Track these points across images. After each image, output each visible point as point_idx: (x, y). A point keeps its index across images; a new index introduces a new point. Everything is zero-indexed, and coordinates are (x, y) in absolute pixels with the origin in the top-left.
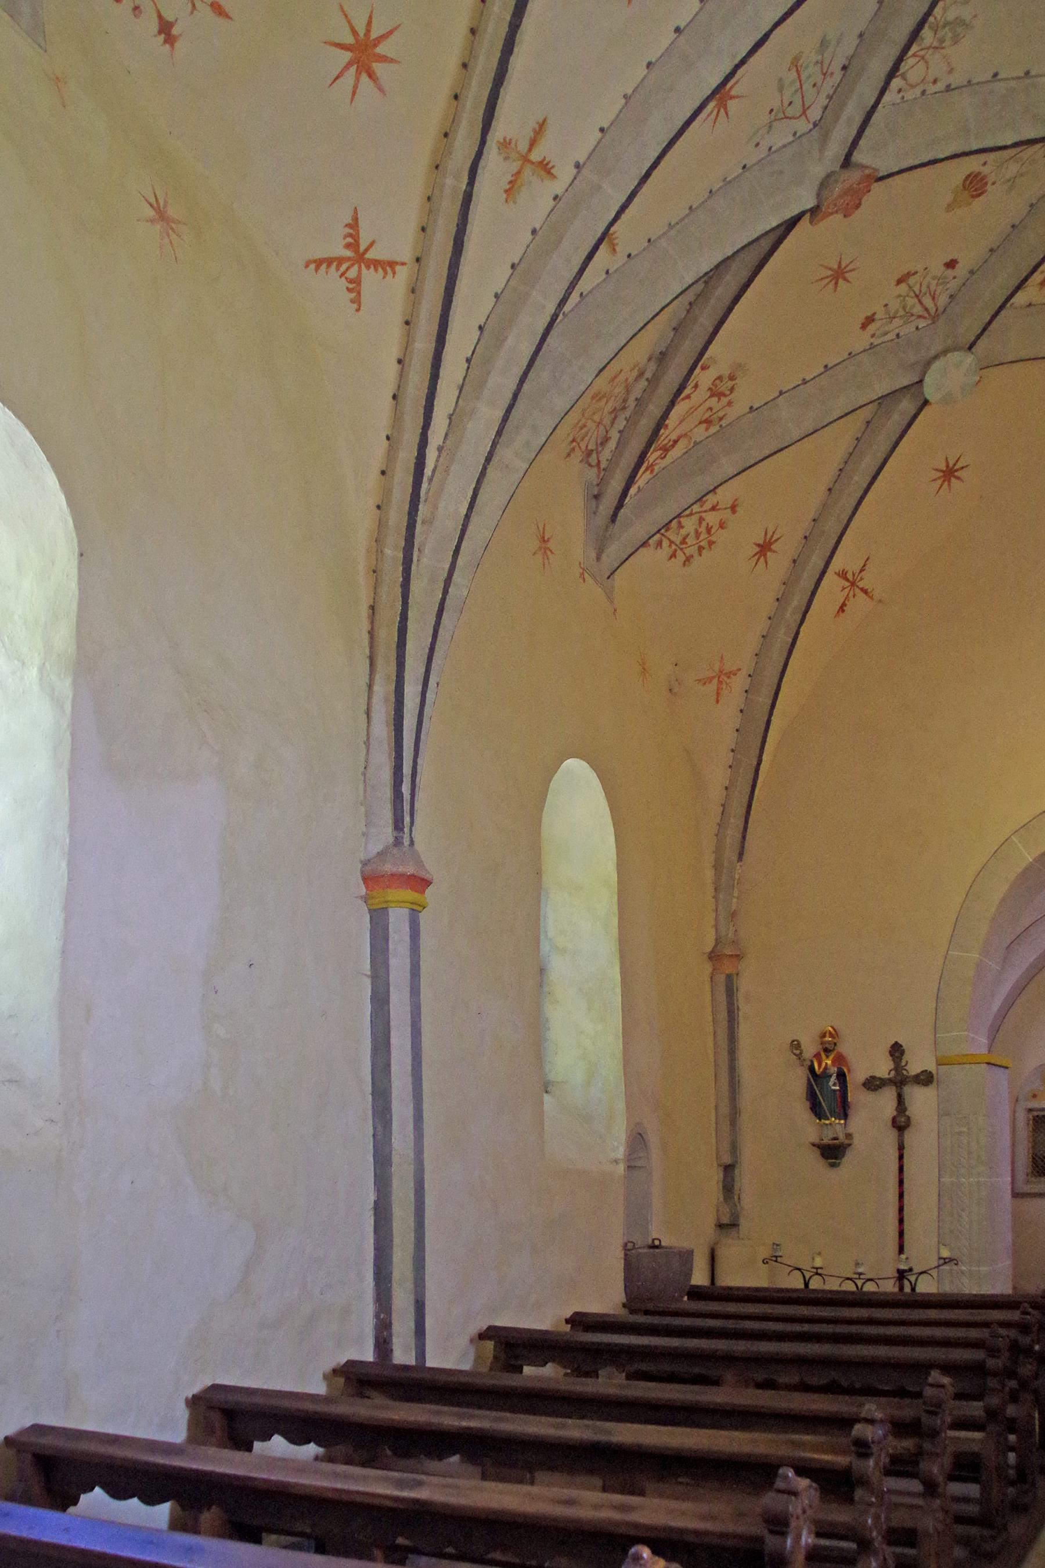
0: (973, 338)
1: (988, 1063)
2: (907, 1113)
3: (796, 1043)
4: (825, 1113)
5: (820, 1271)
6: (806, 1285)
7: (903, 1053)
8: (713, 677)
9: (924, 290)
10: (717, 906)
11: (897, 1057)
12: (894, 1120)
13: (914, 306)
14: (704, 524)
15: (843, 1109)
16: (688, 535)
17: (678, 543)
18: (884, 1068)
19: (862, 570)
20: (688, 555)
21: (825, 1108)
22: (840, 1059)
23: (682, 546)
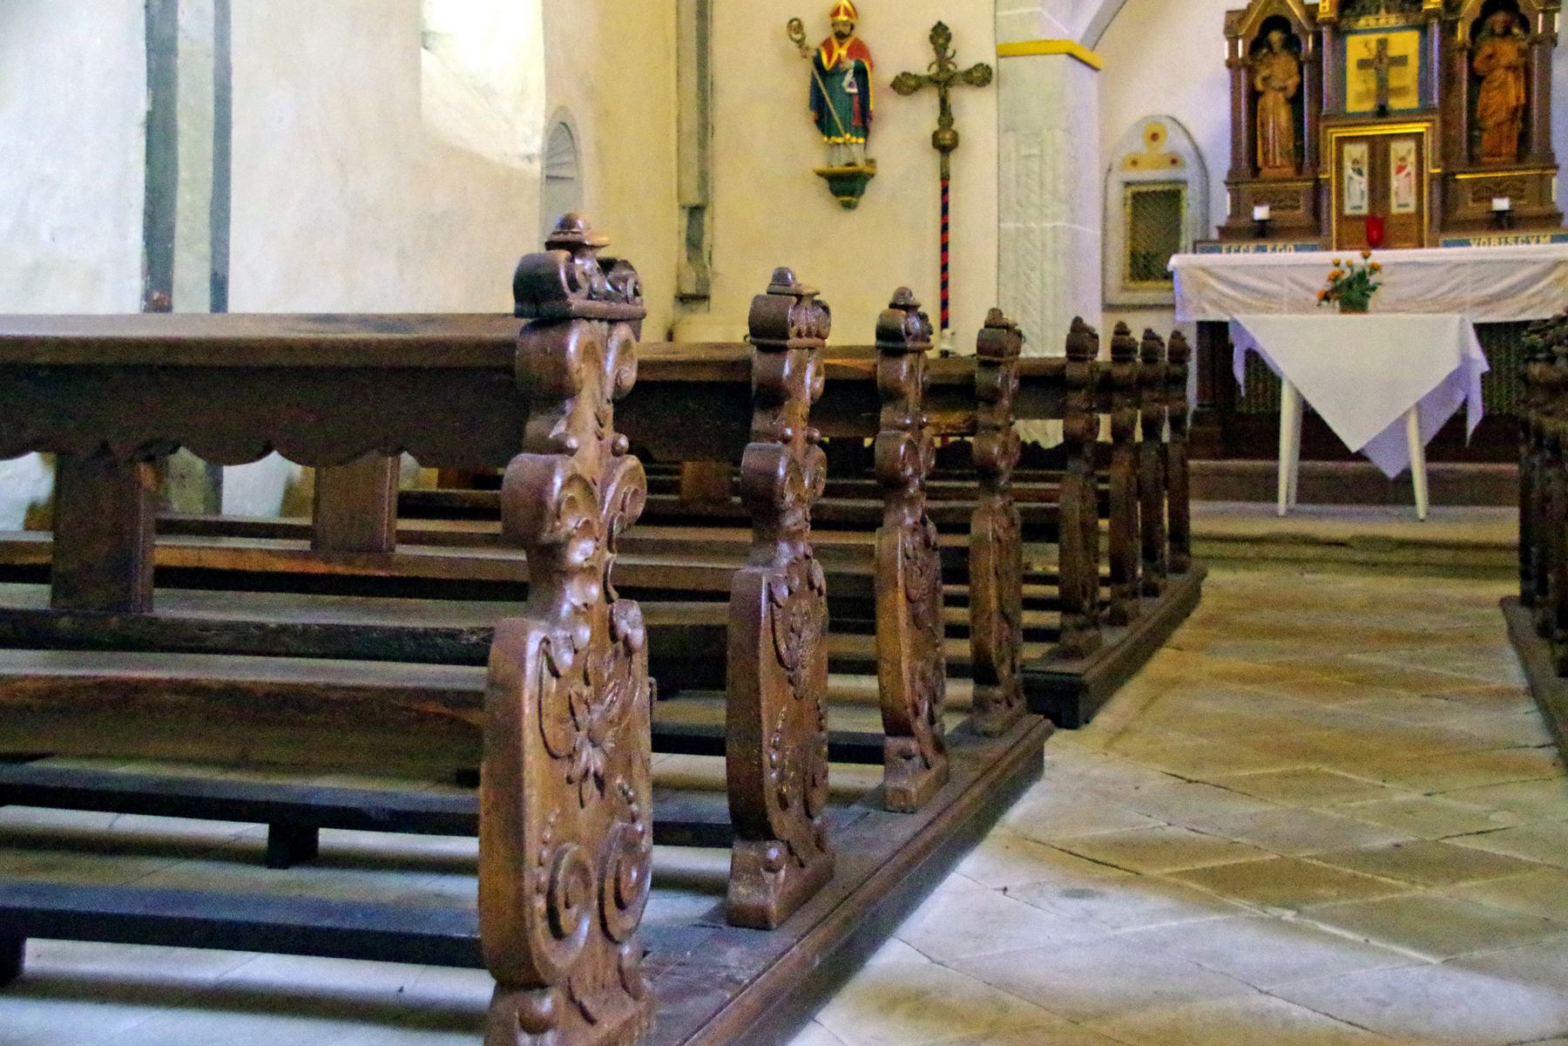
1: (1071, 55)
2: (954, 127)
3: (795, 23)
4: (838, 129)
7: (948, 38)
11: (941, 45)
12: (935, 135)
15: (863, 121)
18: (921, 61)
21: (837, 118)
22: (859, 50)
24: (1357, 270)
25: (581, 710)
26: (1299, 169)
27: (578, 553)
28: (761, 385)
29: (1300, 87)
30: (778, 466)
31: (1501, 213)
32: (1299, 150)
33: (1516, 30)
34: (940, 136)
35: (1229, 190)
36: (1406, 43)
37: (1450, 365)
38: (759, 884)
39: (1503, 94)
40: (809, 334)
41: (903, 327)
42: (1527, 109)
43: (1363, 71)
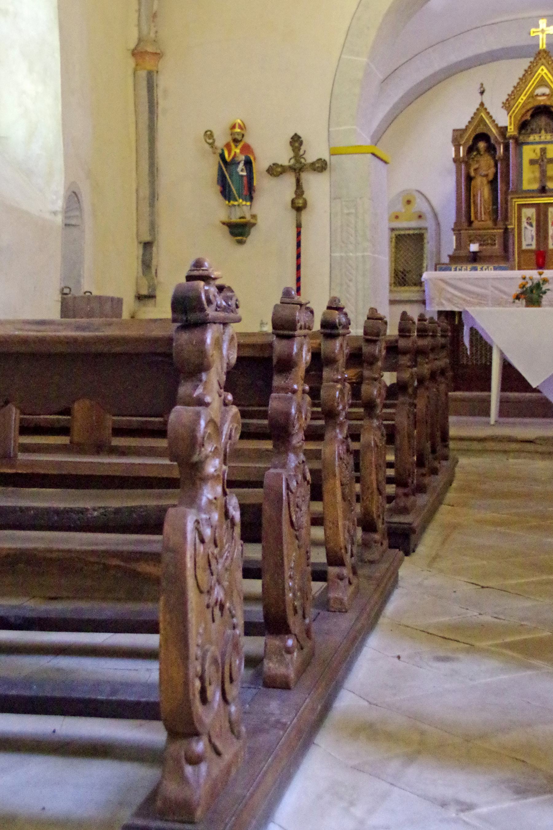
1: (373, 154)
2: (304, 196)
7: (301, 143)
12: (293, 202)
22: (247, 149)
25: (213, 562)
26: (495, 221)
27: (211, 467)
28: (279, 360)
30: (291, 408)
32: (495, 211)
34: (296, 201)
38: (281, 661)
40: (305, 328)
41: (337, 321)
43: (532, 166)
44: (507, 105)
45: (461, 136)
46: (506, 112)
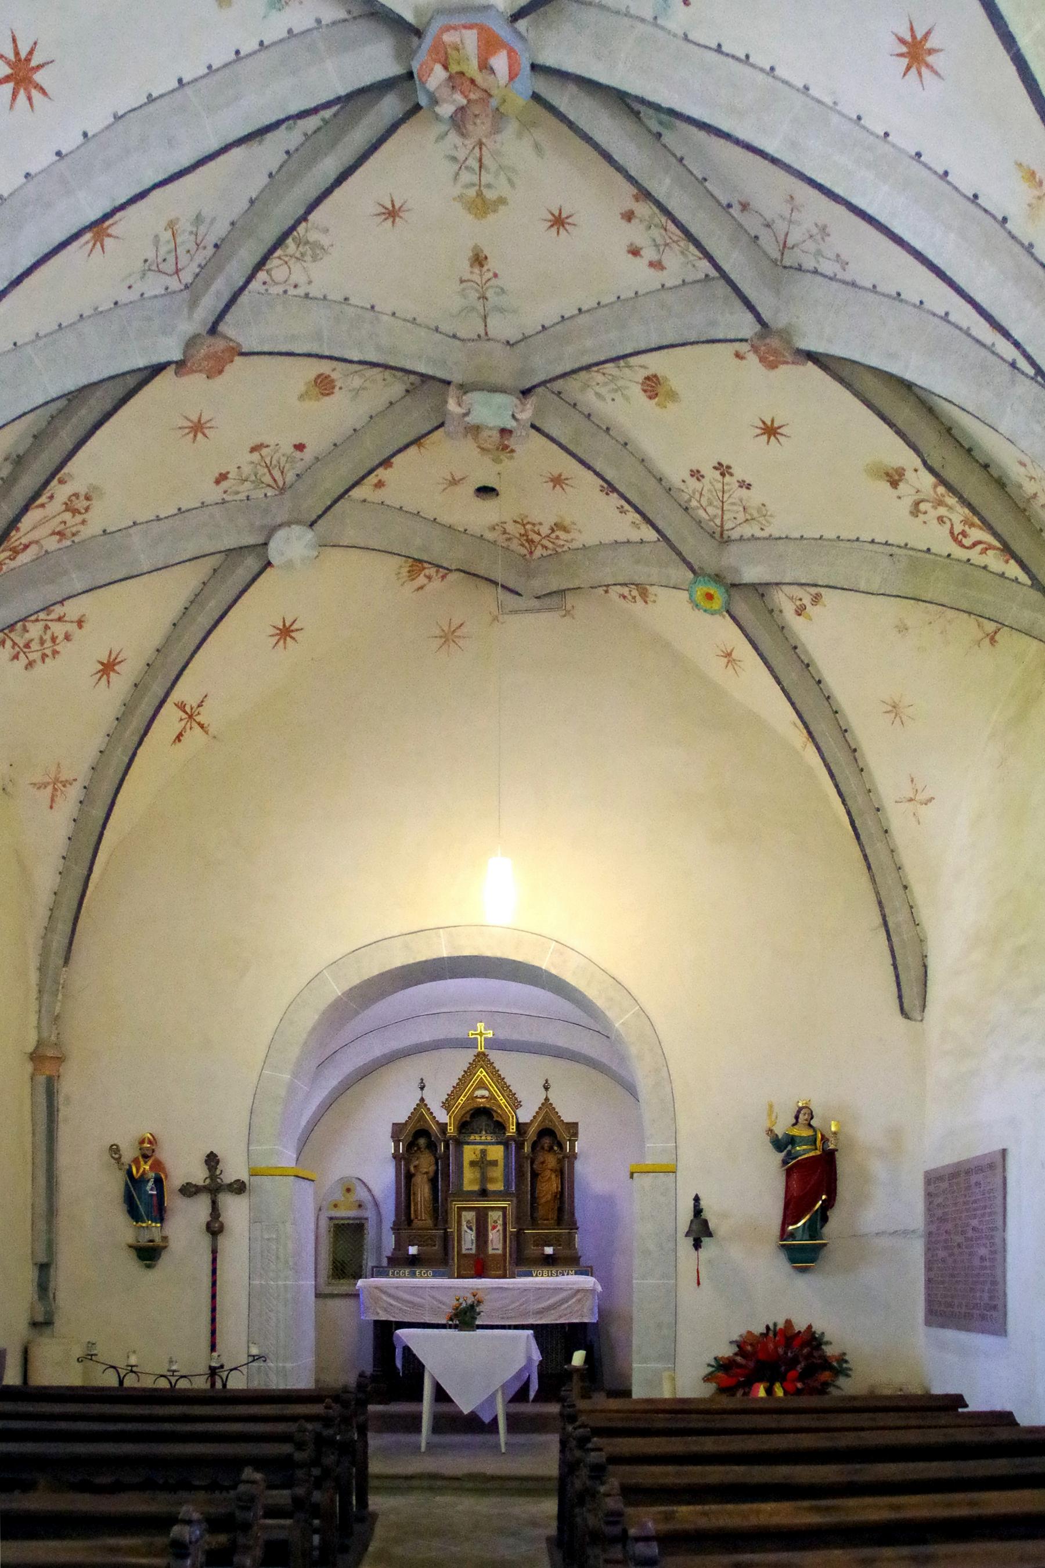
0: (314, 517)
2: (220, 1219)
3: (114, 1147)
4: (142, 1216)
5: (134, 1369)
6: (121, 1382)
7: (218, 1162)
8: (48, 783)
9: (274, 462)
10: (40, 1007)
12: (208, 1226)
13: (265, 474)
14: (49, 632)
15: (160, 1213)
16: (32, 640)
17: (21, 645)
18: (199, 1175)
19: (199, 706)
20: (31, 659)
22: (158, 1165)
23: (25, 650)
24: (469, 1302)
29: (436, 1172)
31: (549, 1256)
32: (435, 1210)
33: (556, 1148)
35: (394, 1233)
36: (496, 1152)
37: (521, 1363)
39: (549, 1186)
42: (562, 1193)
44: (447, 1105)
45: (401, 1131)
46: (446, 1112)
